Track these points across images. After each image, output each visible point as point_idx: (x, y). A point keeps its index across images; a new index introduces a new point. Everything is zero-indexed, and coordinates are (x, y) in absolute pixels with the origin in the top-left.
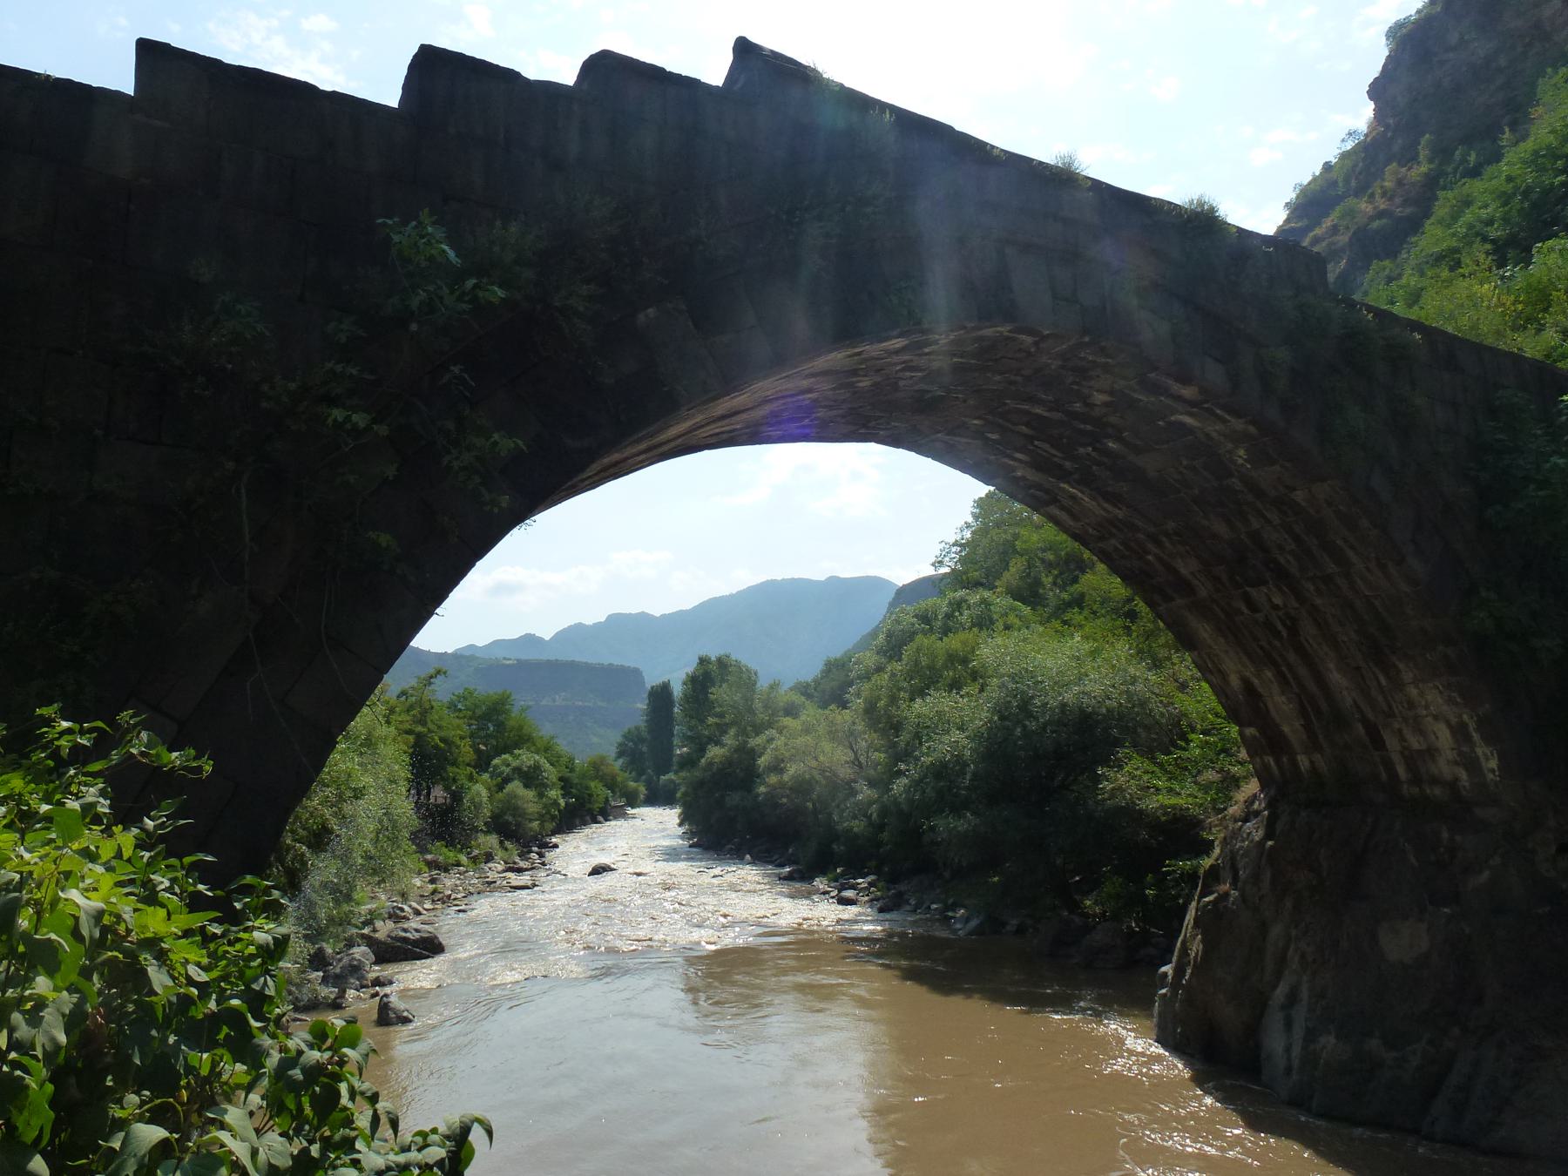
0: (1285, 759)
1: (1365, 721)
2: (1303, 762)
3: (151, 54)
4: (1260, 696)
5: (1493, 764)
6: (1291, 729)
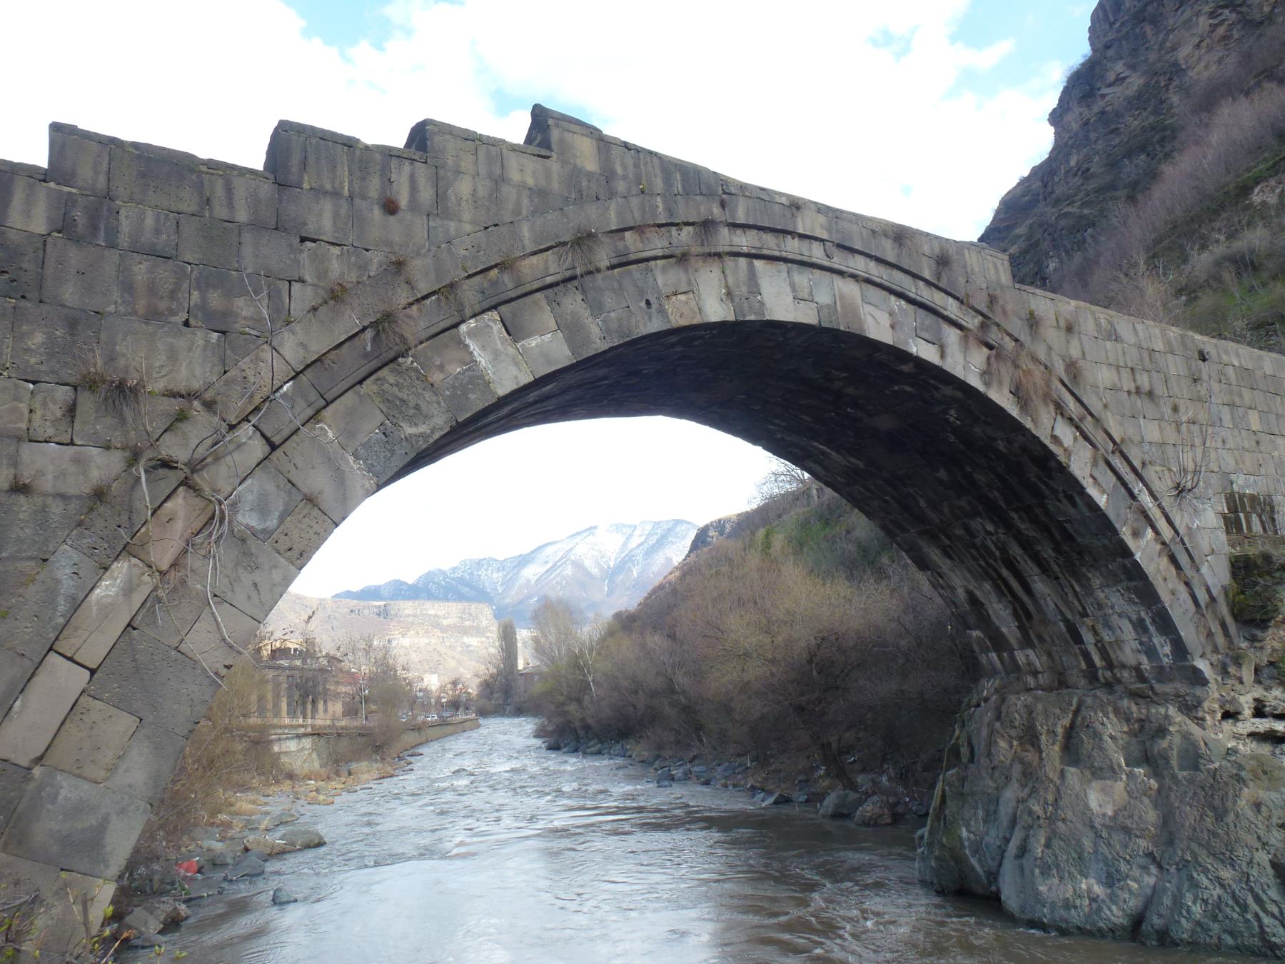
0: (1005, 654)
1: (1066, 620)
2: (1020, 657)
3: (62, 135)
4: (982, 604)
5: (1167, 649)
6: (1009, 628)
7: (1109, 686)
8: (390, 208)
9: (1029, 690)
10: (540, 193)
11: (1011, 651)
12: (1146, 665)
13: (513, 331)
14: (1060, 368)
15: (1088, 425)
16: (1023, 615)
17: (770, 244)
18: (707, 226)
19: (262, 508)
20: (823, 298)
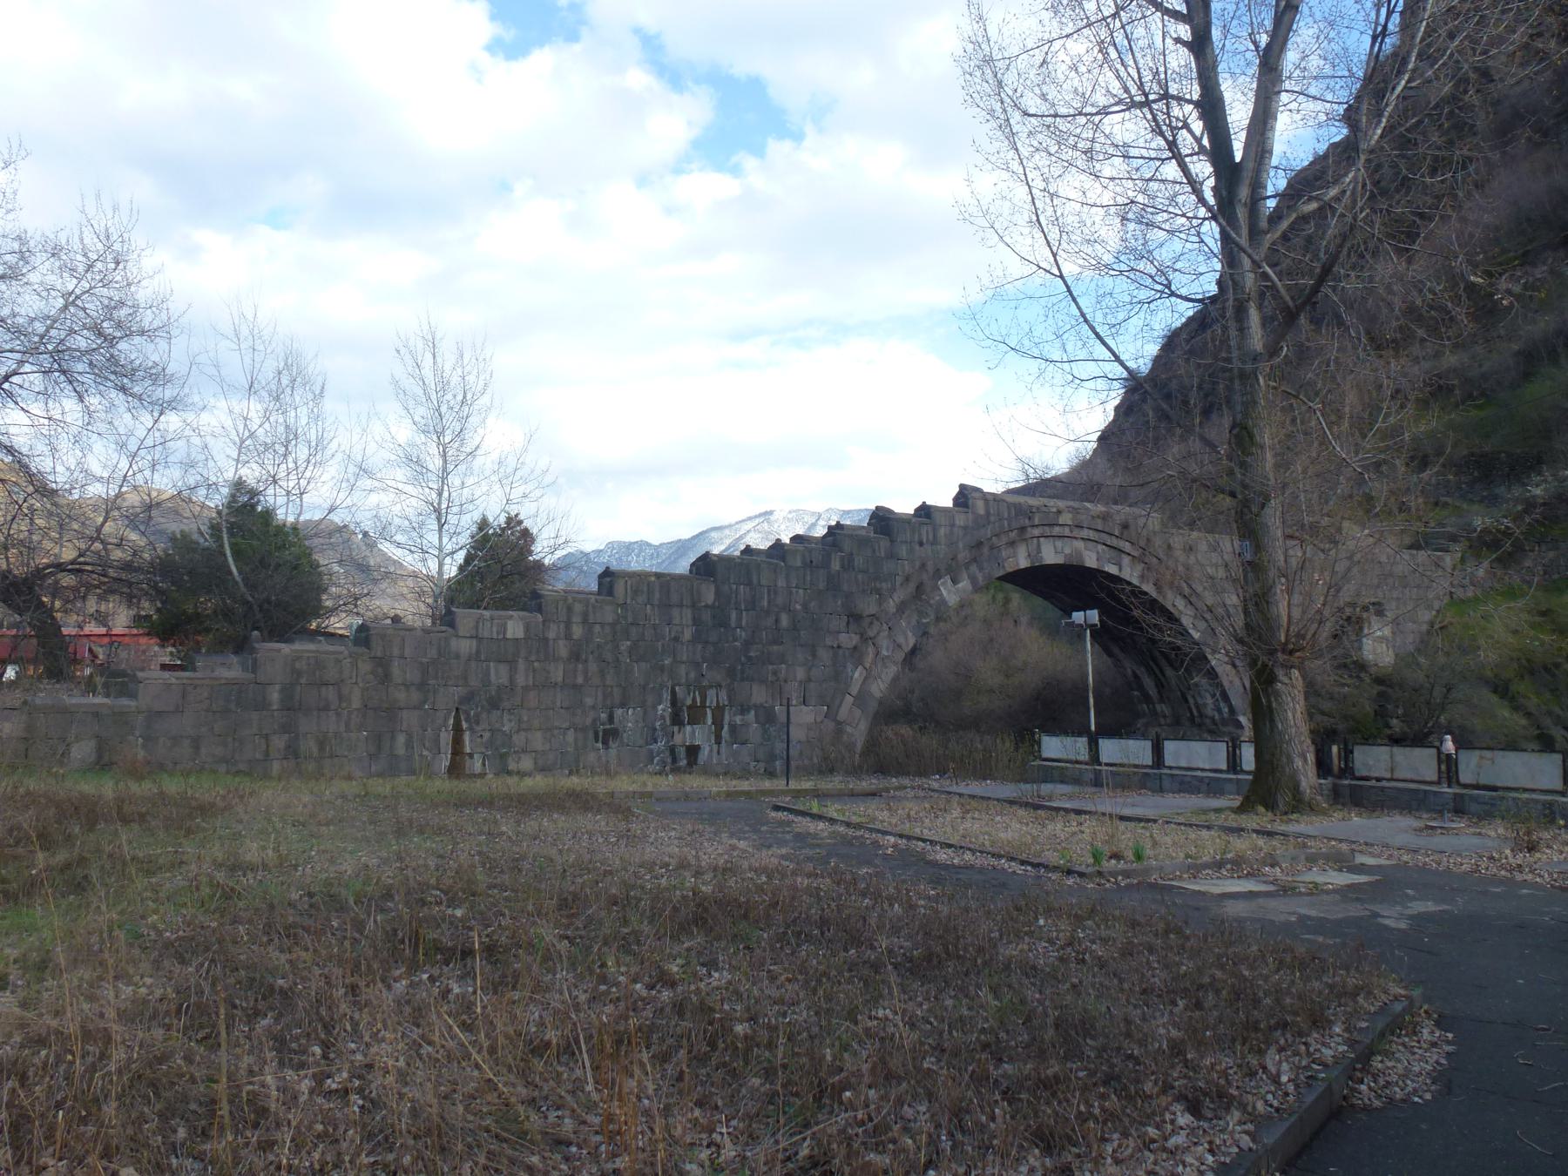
2: (1158, 707)
5: (1226, 710)
6: (1153, 692)
7: (1200, 725)
8: (921, 544)
9: (1160, 725)
10: (965, 528)
11: (1153, 704)
12: (1217, 717)
13: (955, 582)
14: (1180, 568)
15: (1193, 599)
16: (1160, 686)
17: (1047, 530)
18: (1023, 529)
19: (888, 650)
20: (1067, 551)
